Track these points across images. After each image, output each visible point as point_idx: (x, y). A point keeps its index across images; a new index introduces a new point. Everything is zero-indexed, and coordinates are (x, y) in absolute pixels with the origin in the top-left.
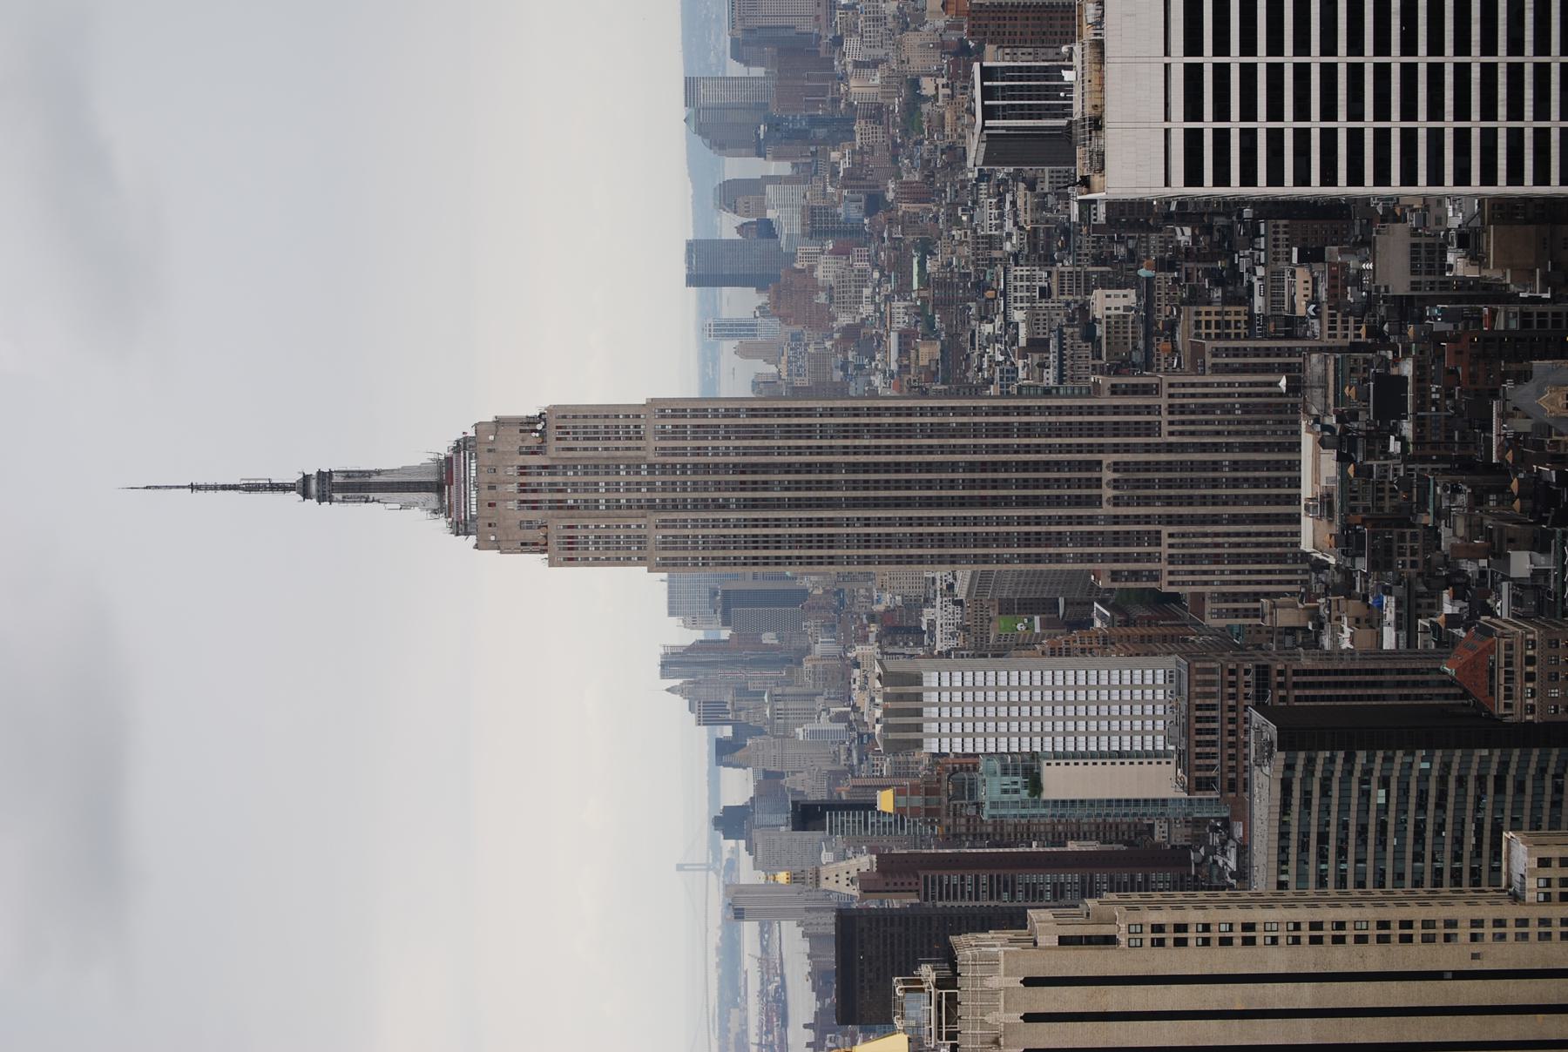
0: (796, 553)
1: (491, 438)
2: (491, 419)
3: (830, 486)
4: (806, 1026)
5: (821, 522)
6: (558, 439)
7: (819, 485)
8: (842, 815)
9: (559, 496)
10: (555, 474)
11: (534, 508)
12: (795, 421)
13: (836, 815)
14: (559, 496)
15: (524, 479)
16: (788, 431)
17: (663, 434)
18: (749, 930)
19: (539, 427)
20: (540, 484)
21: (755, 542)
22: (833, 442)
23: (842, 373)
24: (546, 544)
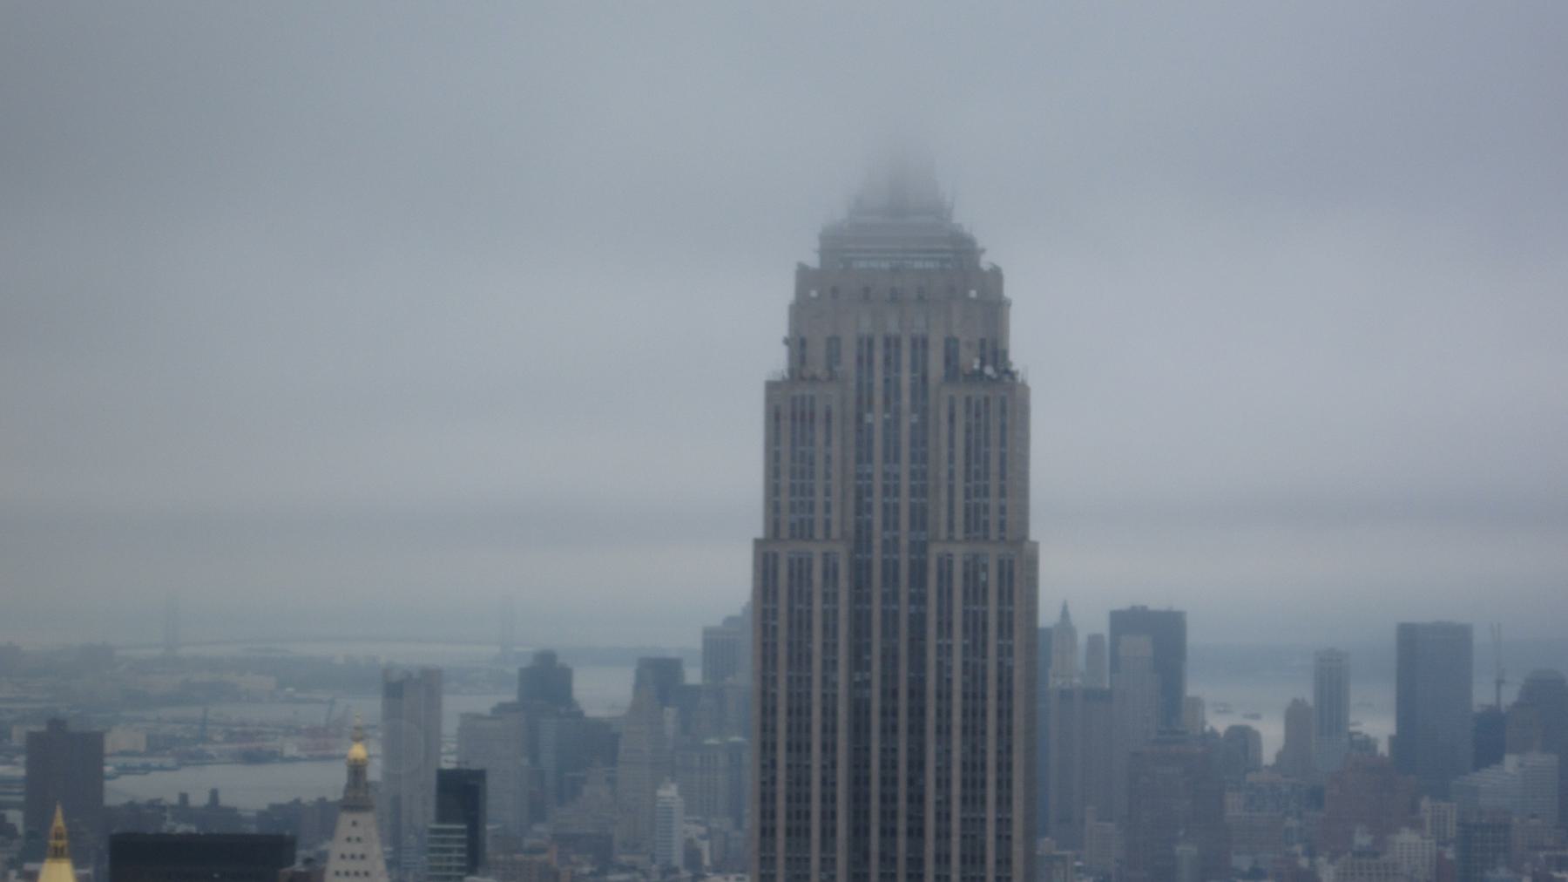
0: (781, 775)
1: (973, 294)
2: (1009, 291)
3: (888, 832)
4: (214, 794)
5: (829, 816)
6: (968, 400)
7: (889, 815)
8: (461, 850)
9: (878, 399)
10: (914, 396)
11: (860, 360)
12: (991, 778)
13: (460, 841)
14: (878, 399)
15: (906, 344)
16: (974, 767)
17: (973, 569)
18: (369, 708)
19: (989, 370)
20: (898, 370)
21: (799, 711)
22: (956, 840)
23: (1246, 868)
24: (802, 378)
